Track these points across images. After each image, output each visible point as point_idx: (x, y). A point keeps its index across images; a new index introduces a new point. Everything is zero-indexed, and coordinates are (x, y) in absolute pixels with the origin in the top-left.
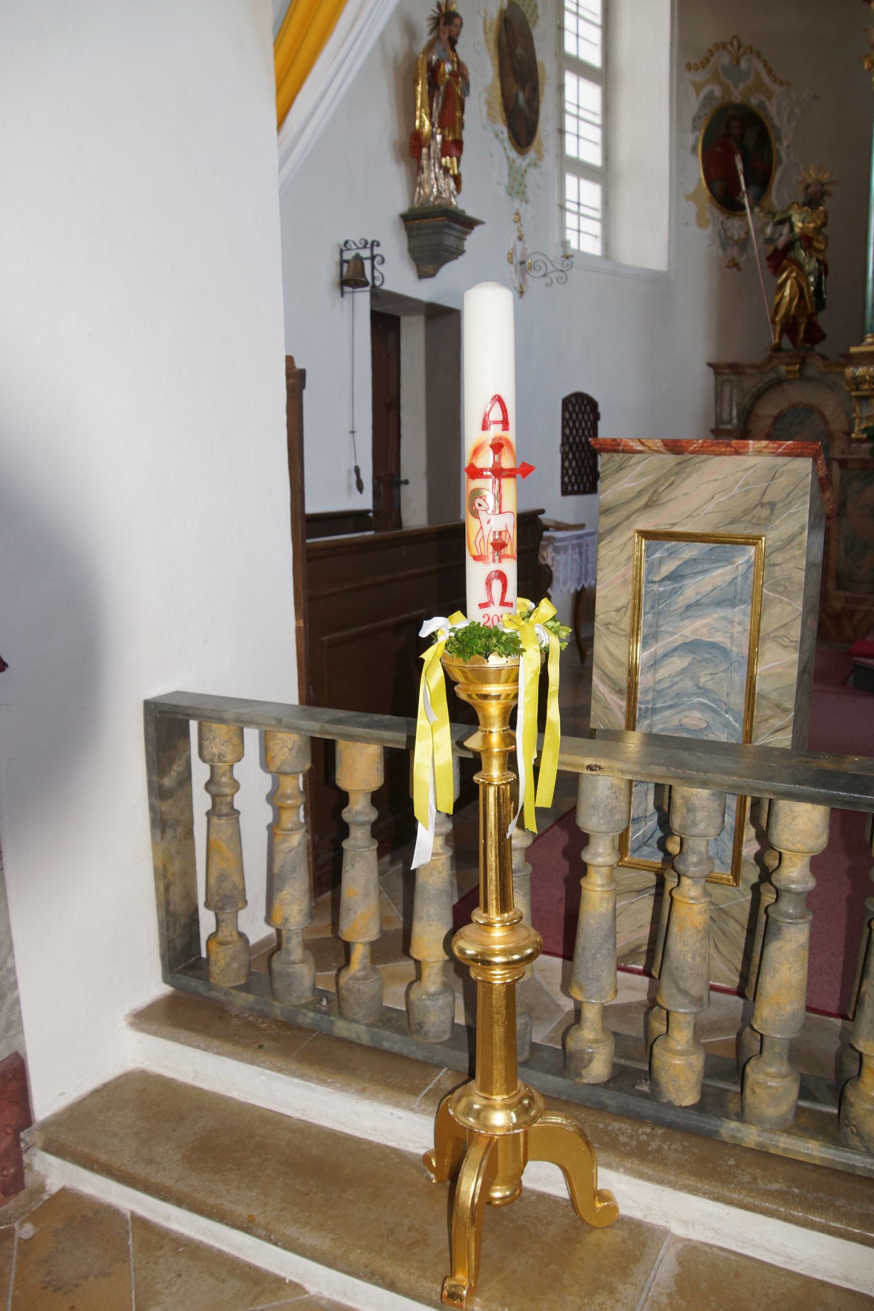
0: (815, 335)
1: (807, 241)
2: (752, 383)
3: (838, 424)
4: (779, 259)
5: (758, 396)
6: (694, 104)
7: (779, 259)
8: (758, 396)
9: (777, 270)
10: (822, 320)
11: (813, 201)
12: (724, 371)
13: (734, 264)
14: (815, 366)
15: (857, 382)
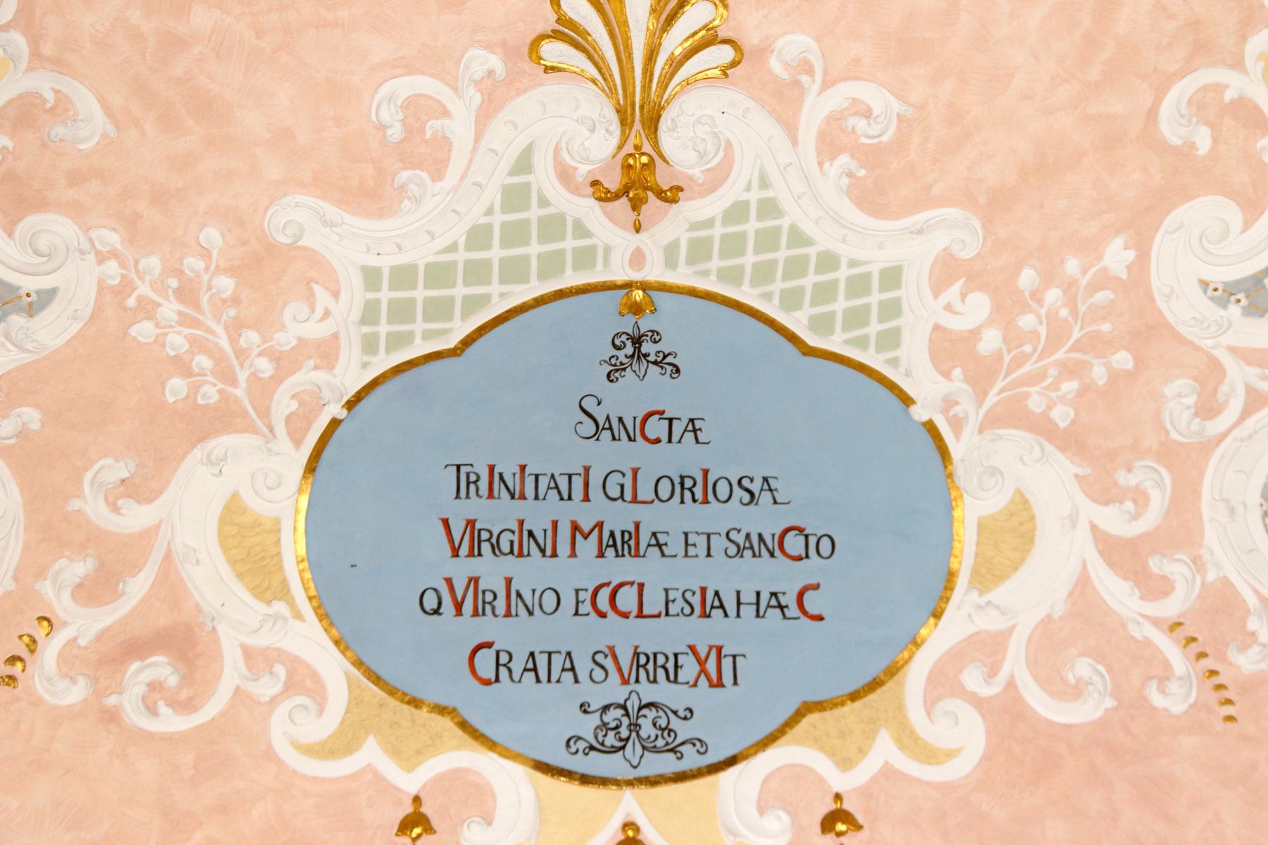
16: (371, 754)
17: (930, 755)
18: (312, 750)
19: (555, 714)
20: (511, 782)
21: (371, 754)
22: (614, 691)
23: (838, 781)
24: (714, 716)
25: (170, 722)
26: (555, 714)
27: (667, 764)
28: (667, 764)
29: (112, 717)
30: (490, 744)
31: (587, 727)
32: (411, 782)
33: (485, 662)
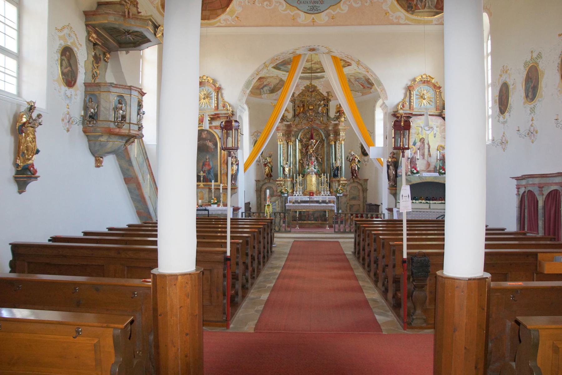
0: (271, 176)
1: (270, 163)
2: (262, 183)
3: (275, 189)
4: (265, 165)
5: (263, 185)
6: (252, 141)
7: (265, 165)
8: (263, 185)
9: (265, 166)
10: (272, 174)
11: (270, 157)
12: (257, 181)
13: (258, 165)
14: (271, 181)
15: (278, 184)
16: (288, 11)
17: (342, 10)
18: (284, 11)
19: (306, 7)
20: (302, 14)
21: (288, 11)
22: (312, 5)
23: (333, 13)
24: (322, 7)
25: (269, 8)
26: (306, 7)
27: (317, 12)
28: (317, 12)
29: (264, 7)
30: (299, 10)
31: (309, 8)
32: (292, 14)
33: (299, 2)
